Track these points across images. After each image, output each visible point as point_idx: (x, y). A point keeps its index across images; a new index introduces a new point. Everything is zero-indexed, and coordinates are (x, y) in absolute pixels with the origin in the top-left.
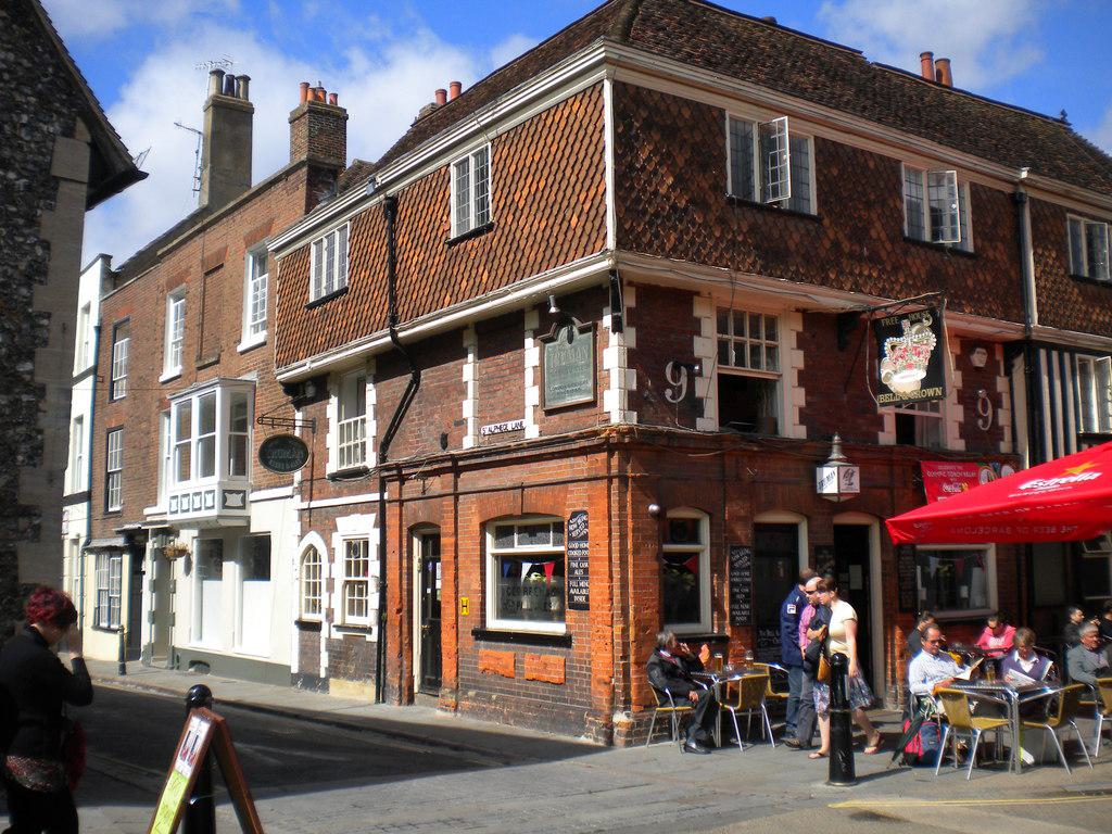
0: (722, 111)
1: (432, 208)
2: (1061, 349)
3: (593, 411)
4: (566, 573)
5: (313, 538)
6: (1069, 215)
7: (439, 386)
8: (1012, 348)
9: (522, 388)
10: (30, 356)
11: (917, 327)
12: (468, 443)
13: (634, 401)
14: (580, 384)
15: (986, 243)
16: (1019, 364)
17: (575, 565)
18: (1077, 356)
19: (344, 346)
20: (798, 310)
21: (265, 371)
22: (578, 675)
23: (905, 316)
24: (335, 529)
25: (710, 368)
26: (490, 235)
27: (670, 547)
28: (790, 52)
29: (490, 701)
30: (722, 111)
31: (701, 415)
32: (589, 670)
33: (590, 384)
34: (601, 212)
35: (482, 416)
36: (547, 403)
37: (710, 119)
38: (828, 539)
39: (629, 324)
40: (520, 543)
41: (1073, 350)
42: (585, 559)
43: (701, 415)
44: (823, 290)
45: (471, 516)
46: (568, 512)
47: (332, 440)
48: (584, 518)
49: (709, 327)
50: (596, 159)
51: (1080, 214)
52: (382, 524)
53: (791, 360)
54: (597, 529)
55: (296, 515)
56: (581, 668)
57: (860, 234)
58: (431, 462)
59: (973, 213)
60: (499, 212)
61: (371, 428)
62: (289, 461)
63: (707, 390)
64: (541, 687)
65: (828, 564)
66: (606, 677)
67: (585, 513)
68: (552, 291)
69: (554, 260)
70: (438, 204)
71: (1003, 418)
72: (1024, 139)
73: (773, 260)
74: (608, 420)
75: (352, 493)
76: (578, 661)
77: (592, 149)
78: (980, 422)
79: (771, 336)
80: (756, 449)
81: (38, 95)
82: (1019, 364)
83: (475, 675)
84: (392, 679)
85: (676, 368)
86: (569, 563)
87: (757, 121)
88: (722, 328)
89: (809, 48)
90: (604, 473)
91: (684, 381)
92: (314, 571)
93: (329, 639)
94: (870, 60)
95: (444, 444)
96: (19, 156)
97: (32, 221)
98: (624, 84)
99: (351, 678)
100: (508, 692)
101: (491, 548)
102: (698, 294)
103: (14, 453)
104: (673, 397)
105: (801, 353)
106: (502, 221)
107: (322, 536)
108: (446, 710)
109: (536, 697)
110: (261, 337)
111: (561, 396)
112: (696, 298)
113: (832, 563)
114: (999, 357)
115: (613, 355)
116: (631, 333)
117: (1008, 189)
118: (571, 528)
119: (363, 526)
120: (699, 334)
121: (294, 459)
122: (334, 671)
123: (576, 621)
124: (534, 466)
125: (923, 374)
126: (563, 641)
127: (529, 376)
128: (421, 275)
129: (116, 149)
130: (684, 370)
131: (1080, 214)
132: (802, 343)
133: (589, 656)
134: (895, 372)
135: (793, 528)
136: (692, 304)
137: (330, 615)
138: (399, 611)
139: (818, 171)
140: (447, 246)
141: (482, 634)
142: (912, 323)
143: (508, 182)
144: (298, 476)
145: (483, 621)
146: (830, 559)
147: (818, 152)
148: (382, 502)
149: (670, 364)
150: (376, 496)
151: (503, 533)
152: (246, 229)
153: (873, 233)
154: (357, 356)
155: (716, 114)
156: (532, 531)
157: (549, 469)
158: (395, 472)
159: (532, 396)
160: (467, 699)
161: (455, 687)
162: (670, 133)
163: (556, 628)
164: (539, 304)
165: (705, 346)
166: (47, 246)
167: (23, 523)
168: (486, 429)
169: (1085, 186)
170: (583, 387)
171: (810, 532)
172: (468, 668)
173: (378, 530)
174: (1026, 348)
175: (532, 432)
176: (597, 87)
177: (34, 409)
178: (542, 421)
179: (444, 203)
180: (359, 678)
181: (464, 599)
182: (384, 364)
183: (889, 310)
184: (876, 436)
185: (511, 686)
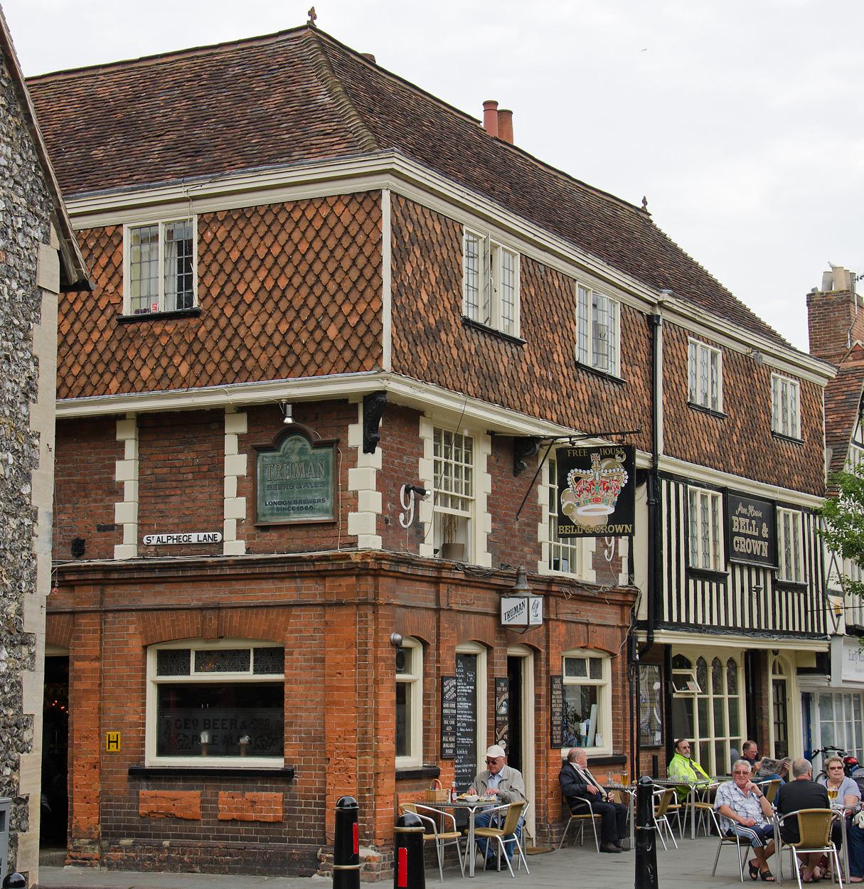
11: (607, 462)
12: (125, 552)
13: (385, 524)
14: (313, 501)
15: (629, 369)
20: (488, 433)
22: (302, 811)
23: (596, 450)
26: (193, 322)
29: (160, 848)
40: (197, 670)
41: (686, 481)
57: (546, 360)
73: (488, 387)
74: (353, 543)
76: (304, 797)
78: (606, 552)
85: (407, 491)
98: (398, 195)
100: (188, 837)
102: (422, 413)
104: (405, 522)
105: (490, 476)
108: (83, 865)
111: (283, 512)
117: (647, 310)
124: (238, 586)
125: (612, 510)
126: (284, 776)
127: (230, 486)
134: (578, 504)
136: (418, 424)
141: (141, 774)
142: (603, 458)
146: (505, 692)
153: (555, 356)
157: (262, 590)
159: (235, 507)
162: (426, 249)
164: (262, 414)
167: (25, 649)
170: (318, 505)
172: (119, 814)
175: (235, 548)
178: (249, 538)
179: (110, 270)
181: (113, 735)
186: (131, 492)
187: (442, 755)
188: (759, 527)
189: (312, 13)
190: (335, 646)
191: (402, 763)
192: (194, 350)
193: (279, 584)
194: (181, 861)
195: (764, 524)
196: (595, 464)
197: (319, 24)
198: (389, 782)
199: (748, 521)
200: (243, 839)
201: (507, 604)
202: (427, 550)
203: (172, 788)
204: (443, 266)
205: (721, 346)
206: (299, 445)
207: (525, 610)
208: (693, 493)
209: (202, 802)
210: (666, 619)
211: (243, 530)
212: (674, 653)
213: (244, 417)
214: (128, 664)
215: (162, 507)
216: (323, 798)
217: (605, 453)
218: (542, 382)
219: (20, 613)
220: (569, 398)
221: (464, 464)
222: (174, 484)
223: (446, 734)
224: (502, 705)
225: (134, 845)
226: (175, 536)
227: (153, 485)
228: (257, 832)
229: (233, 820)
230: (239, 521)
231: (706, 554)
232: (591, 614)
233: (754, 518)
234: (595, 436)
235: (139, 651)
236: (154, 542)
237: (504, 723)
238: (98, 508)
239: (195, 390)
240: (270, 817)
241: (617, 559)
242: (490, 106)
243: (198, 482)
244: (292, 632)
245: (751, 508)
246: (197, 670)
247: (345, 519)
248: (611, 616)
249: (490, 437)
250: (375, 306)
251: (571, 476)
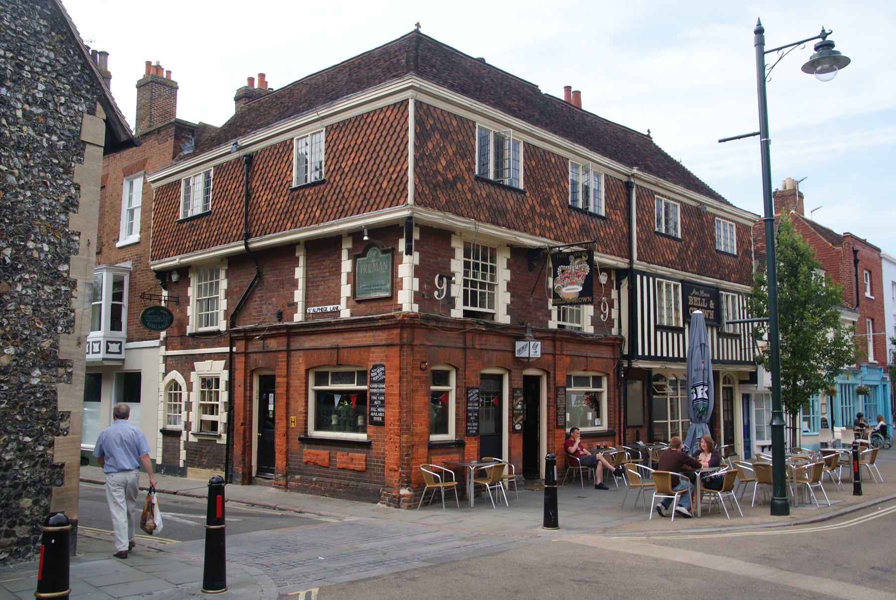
0: (474, 123)
1: (278, 166)
2: (648, 275)
3: (390, 303)
4: (368, 404)
5: (175, 375)
6: (656, 196)
7: (277, 280)
8: (620, 274)
9: (339, 286)
10: (67, 261)
12: (298, 318)
13: (418, 297)
14: (382, 285)
15: (612, 211)
16: (625, 283)
17: (374, 398)
18: (657, 279)
19: (208, 250)
20: (508, 245)
21: (138, 260)
22: (375, 465)
23: (571, 253)
24: (194, 370)
25: (459, 278)
26: (322, 187)
27: (433, 388)
28: (501, 84)
30: (474, 123)
31: (454, 308)
32: (384, 462)
33: (389, 286)
34: (404, 181)
35: (307, 304)
36: (357, 296)
37: (467, 126)
38: (520, 384)
39: (415, 250)
41: (655, 276)
42: (382, 394)
43: (454, 308)
44: (524, 234)
45: (299, 365)
46: (371, 365)
47: (191, 311)
48: (382, 369)
49: (459, 254)
50: (402, 148)
51: (662, 196)
52: (230, 367)
53: (503, 275)
54: (392, 376)
55: (161, 358)
56: (377, 462)
57: (545, 202)
58: (271, 329)
59: (606, 191)
60: (329, 174)
61: (223, 304)
62: (161, 323)
63: (457, 291)
64: (350, 473)
65: (519, 399)
66: (396, 467)
67: (383, 366)
68: (367, 226)
69: (369, 207)
70: (284, 164)
71: (615, 314)
72: (629, 148)
73: (497, 217)
74: (400, 309)
75: (206, 346)
76: (376, 457)
77: (399, 141)
78: (602, 316)
79: (493, 260)
80: (484, 329)
81: (71, 83)
82: (625, 283)
83: (300, 466)
84: (239, 469)
85: (441, 278)
86: (370, 397)
87: (493, 130)
88: (467, 255)
89: (511, 82)
90: (397, 342)
91: (445, 286)
92: (177, 397)
93: (187, 442)
94: (544, 91)
95: (280, 316)
96: (59, 124)
97: (68, 171)
98: (421, 102)
99: (204, 467)
101: (312, 387)
102: (454, 233)
103: (55, 325)
104: (439, 296)
105: (509, 271)
106: (332, 180)
107: (182, 374)
108: (279, 488)
109: (345, 479)
110: (135, 237)
111: (368, 292)
112: (453, 236)
113: (522, 398)
114: (613, 278)
115: (406, 268)
116: (416, 255)
117: (625, 179)
119: (217, 369)
120: (454, 258)
121: (163, 323)
122: (189, 462)
123: (375, 432)
124: (347, 335)
125: (580, 289)
126: (364, 446)
127: (344, 278)
128: (269, 208)
129: (122, 125)
130: (445, 279)
131: (662, 196)
132: (509, 266)
133: (384, 454)
134: (563, 286)
135: (500, 378)
136: (450, 239)
137: (188, 426)
138: (242, 424)
139: (525, 163)
140: (289, 191)
141: (308, 441)
142: (576, 258)
143: (337, 155)
144: (163, 334)
145: (306, 432)
146: (520, 396)
147: (525, 151)
148: (231, 352)
149: (438, 276)
150: (227, 349)
151: (321, 378)
152: (125, 164)
153: (552, 202)
154: (216, 257)
155: (471, 124)
156: (339, 377)
157: (357, 338)
158: (242, 334)
159: (346, 290)
160: (295, 481)
161: (285, 473)
162: (445, 134)
163: (362, 437)
164: (356, 234)
165: (457, 265)
166: (78, 188)
168: (311, 310)
169: (664, 178)
170: (383, 288)
171: (510, 380)
172: (295, 461)
173: (226, 372)
174: (629, 273)
176: (405, 103)
177: (69, 296)
179: (288, 163)
180: (210, 468)
182: (234, 262)
183: (561, 249)
184: (547, 323)
185: (326, 472)
186: (301, 284)
187: (468, 433)
188: (708, 302)
189: (418, 25)
190: (390, 370)
191: (435, 438)
192: (322, 201)
194: (320, 489)
195: (711, 301)
196: (572, 262)
197: (422, 31)
198: (423, 451)
199: (699, 299)
200: (348, 479)
201: (519, 345)
202: (457, 313)
203: (317, 449)
204: (459, 145)
205: (679, 201)
206: (375, 253)
207: (528, 348)
208: (660, 284)
210: (640, 353)
211: (350, 303)
212: (654, 373)
213: (350, 239)
215: (315, 292)
216: (384, 458)
217: (577, 255)
218: (541, 215)
219: (55, 346)
220: (564, 226)
221: (489, 264)
223: (470, 421)
224: (518, 404)
225: (301, 479)
226: (320, 307)
228: (355, 476)
229: (343, 468)
231: (670, 317)
232: (590, 351)
233: (704, 297)
234: (572, 245)
235: (303, 373)
236: (311, 312)
237: (520, 414)
239: (322, 224)
241: (610, 322)
242: (568, 89)
243: (332, 277)
245: (702, 292)
248: (606, 352)
249: (509, 248)
250: (405, 167)
251: (559, 270)
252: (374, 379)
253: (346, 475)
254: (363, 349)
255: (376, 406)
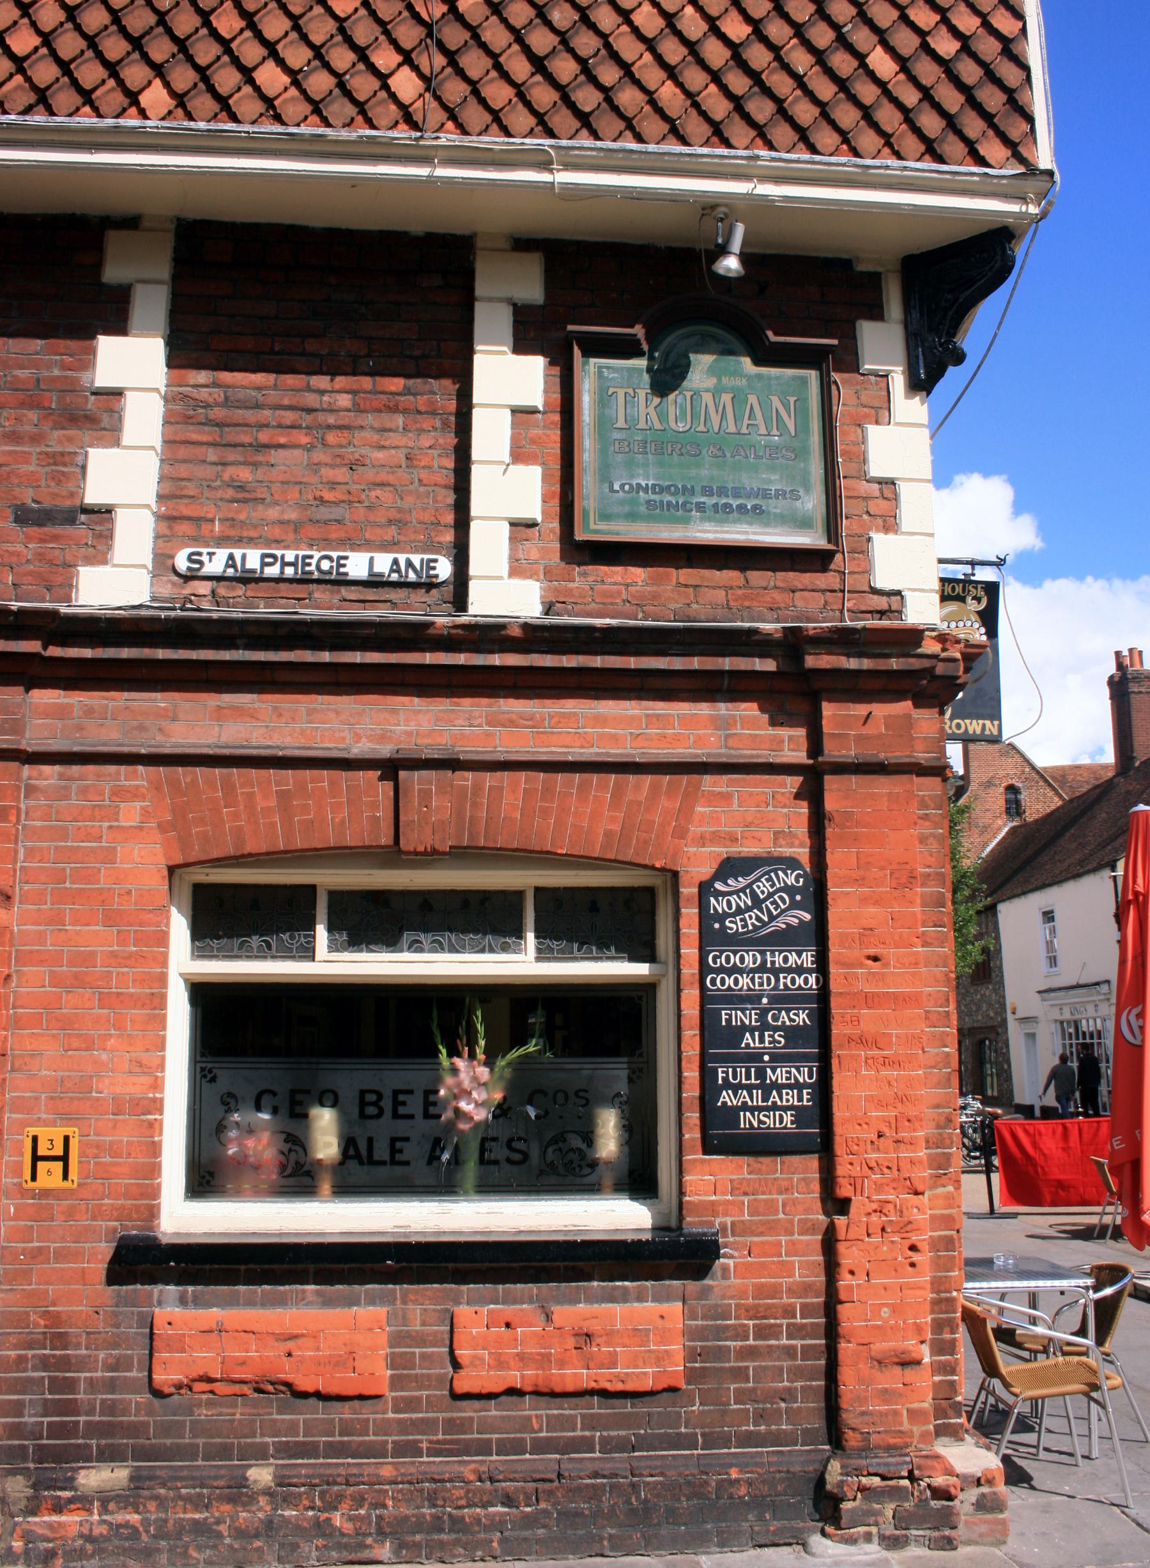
14: (765, 494)
22: (750, 1353)
109: (517, 1447)
111: (679, 513)
118: (718, 905)
145: (153, 1213)
190: (859, 881)
193: (660, 708)
194: (322, 1528)
200: (540, 1446)
209: (397, 1339)
211: (532, 550)
214: (111, 918)
215: (245, 474)
222: (289, 417)
227: (218, 413)
228: (591, 1423)
229: (512, 1392)
230: (520, 527)
238: (25, 458)
240: (646, 1376)
243: (370, 419)
244: (702, 840)
246: (333, 947)
247: (863, 549)
252: (733, 926)
253: (525, 1424)
254: (647, 780)
255: (756, 1057)
